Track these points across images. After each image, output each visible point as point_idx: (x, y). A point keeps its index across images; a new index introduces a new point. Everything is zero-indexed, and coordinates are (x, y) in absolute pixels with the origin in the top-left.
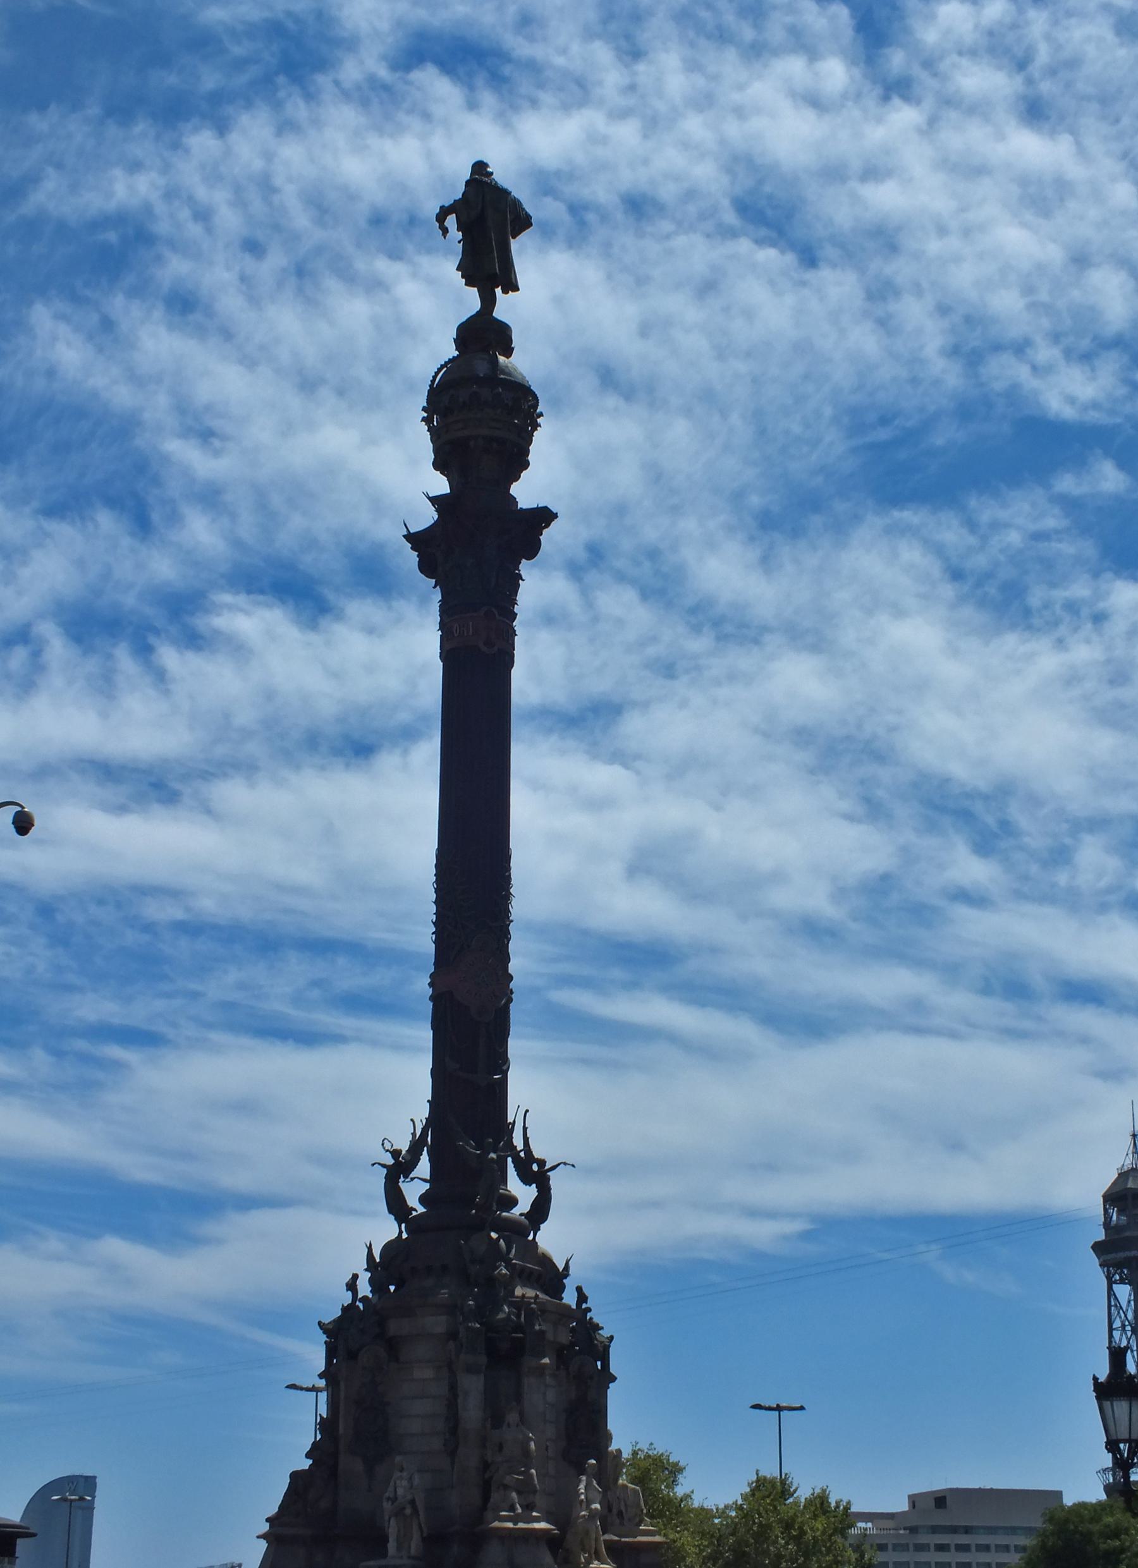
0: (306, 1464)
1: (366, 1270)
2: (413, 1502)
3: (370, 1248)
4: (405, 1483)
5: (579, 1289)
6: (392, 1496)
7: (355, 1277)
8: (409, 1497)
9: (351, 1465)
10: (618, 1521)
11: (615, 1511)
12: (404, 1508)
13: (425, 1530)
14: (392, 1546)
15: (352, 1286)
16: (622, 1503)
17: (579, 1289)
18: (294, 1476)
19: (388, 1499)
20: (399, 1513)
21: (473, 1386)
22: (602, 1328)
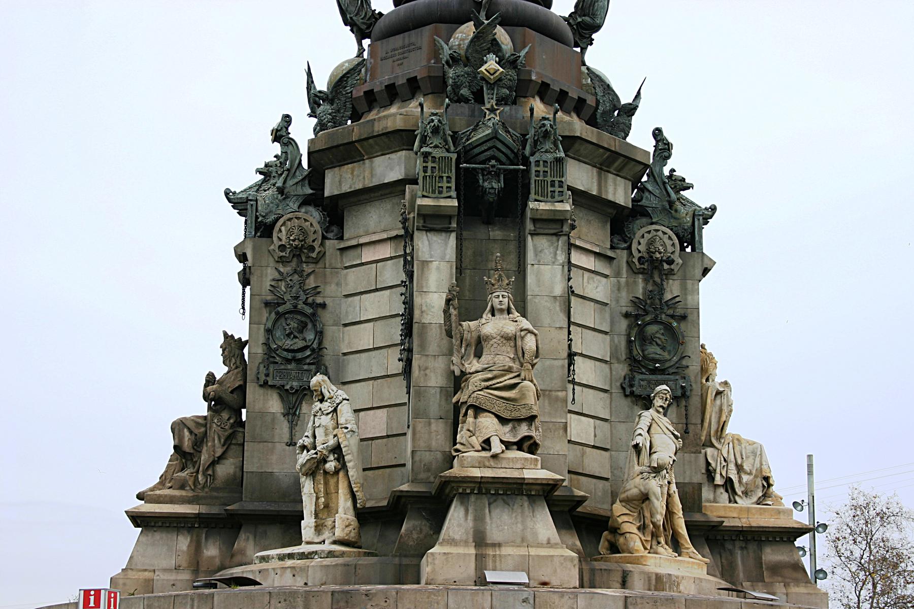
0: (201, 409)
1: (311, 116)
2: (337, 450)
3: (309, 74)
4: (326, 420)
5: (657, 133)
6: (307, 442)
7: (287, 120)
8: (332, 442)
9: (265, 404)
10: (725, 496)
11: (718, 480)
12: (325, 461)
13: (359, 495)
14: (308, 524)
15: (280, 135)
16: (732, 466)
17: (657, 133)
18: (178, 427)
19: (303, 447)
20: (315, 469)
21: (437, 254)
22: (688, 187)
